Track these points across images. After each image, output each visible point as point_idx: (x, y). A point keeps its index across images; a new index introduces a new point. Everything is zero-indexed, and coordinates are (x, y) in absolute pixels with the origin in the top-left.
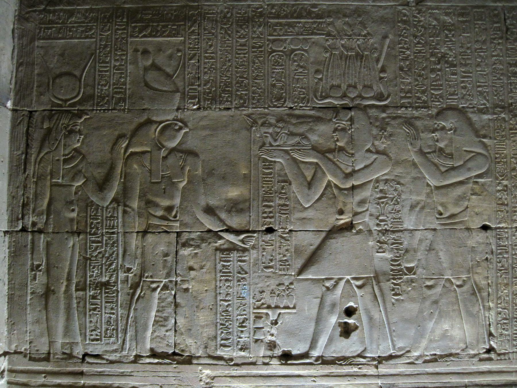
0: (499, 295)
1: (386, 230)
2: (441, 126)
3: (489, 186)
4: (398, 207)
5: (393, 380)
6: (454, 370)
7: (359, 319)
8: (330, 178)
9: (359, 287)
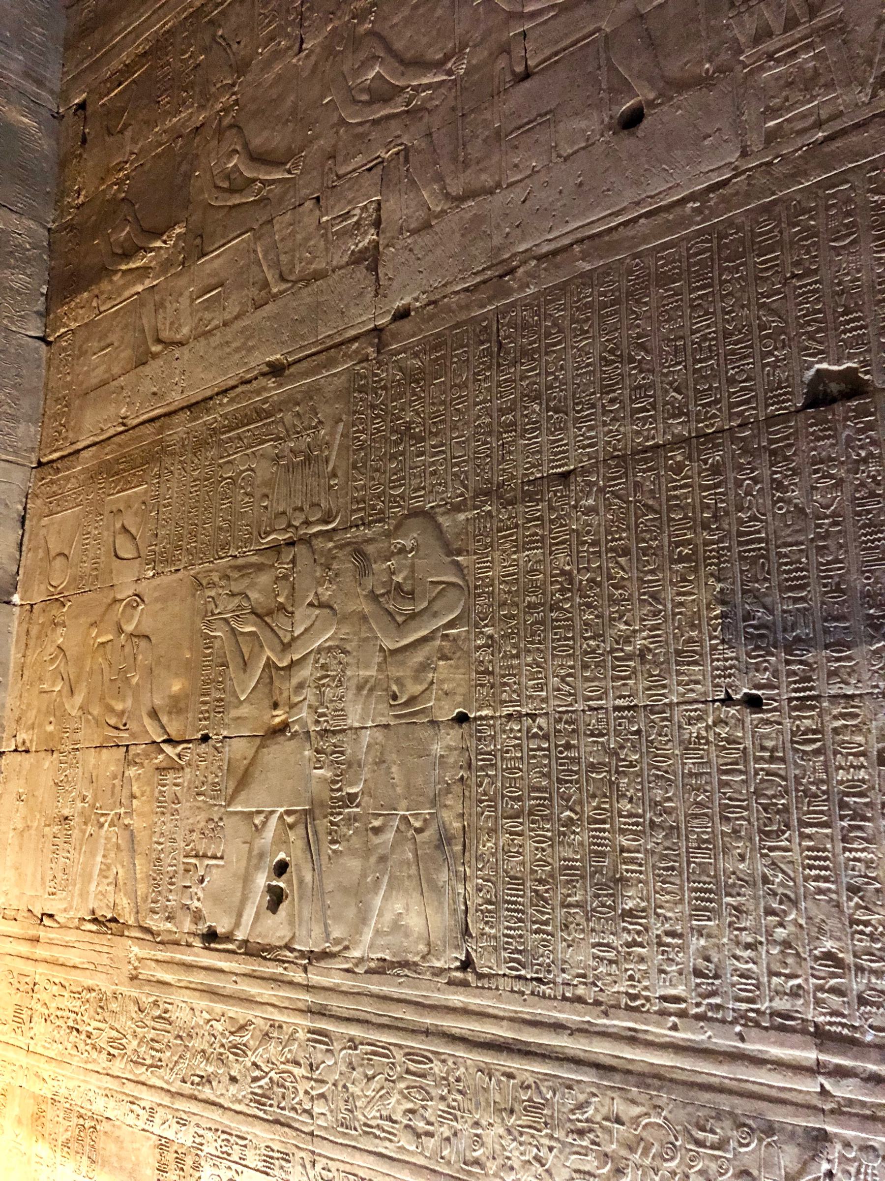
0: (480, 852)
1: (326, 731)
4: (341, 691)
5: (326, 999)
7: (289, 882)
8: (269, 653)
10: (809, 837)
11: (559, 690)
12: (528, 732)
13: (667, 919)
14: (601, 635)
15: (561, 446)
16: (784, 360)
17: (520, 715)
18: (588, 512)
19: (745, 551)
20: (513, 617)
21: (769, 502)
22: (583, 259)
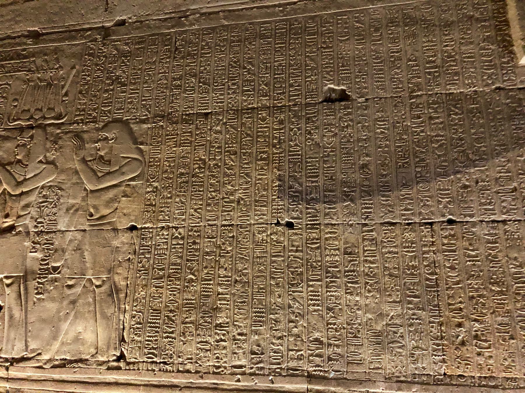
0: (136, 297)
1: (42, 231)
2: (104, 136)
3: (140, 188)
4: (54, 210)
6: (80, 378)
8: (5, 186)
9: (8, 286)
10: (312, 286)
11: (193, 215)
12: (172, 236)
13: (240, 327)
14: (217, 191)
15: (205, 100)
16: (315, 80)
17: (169, 227)
18: (217, 133)
19: (292, 159)
20: (171, 178)
21: (304, 139)
22: (224, 19)
